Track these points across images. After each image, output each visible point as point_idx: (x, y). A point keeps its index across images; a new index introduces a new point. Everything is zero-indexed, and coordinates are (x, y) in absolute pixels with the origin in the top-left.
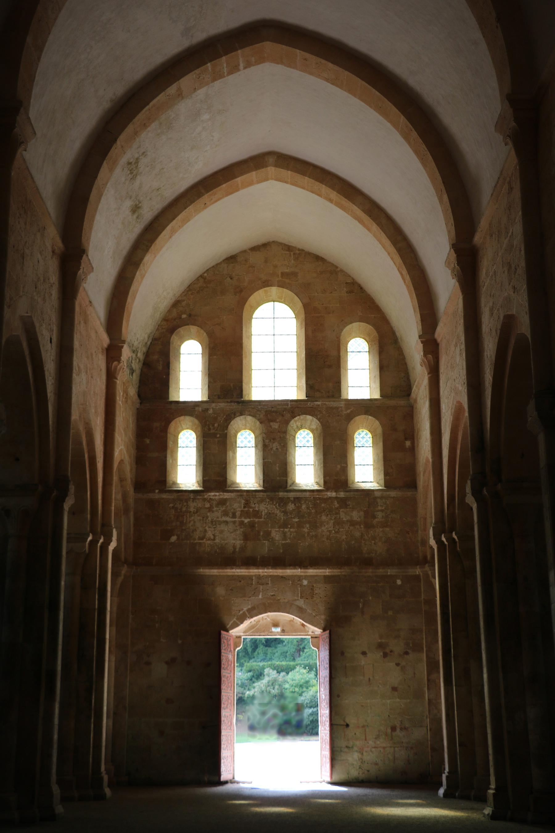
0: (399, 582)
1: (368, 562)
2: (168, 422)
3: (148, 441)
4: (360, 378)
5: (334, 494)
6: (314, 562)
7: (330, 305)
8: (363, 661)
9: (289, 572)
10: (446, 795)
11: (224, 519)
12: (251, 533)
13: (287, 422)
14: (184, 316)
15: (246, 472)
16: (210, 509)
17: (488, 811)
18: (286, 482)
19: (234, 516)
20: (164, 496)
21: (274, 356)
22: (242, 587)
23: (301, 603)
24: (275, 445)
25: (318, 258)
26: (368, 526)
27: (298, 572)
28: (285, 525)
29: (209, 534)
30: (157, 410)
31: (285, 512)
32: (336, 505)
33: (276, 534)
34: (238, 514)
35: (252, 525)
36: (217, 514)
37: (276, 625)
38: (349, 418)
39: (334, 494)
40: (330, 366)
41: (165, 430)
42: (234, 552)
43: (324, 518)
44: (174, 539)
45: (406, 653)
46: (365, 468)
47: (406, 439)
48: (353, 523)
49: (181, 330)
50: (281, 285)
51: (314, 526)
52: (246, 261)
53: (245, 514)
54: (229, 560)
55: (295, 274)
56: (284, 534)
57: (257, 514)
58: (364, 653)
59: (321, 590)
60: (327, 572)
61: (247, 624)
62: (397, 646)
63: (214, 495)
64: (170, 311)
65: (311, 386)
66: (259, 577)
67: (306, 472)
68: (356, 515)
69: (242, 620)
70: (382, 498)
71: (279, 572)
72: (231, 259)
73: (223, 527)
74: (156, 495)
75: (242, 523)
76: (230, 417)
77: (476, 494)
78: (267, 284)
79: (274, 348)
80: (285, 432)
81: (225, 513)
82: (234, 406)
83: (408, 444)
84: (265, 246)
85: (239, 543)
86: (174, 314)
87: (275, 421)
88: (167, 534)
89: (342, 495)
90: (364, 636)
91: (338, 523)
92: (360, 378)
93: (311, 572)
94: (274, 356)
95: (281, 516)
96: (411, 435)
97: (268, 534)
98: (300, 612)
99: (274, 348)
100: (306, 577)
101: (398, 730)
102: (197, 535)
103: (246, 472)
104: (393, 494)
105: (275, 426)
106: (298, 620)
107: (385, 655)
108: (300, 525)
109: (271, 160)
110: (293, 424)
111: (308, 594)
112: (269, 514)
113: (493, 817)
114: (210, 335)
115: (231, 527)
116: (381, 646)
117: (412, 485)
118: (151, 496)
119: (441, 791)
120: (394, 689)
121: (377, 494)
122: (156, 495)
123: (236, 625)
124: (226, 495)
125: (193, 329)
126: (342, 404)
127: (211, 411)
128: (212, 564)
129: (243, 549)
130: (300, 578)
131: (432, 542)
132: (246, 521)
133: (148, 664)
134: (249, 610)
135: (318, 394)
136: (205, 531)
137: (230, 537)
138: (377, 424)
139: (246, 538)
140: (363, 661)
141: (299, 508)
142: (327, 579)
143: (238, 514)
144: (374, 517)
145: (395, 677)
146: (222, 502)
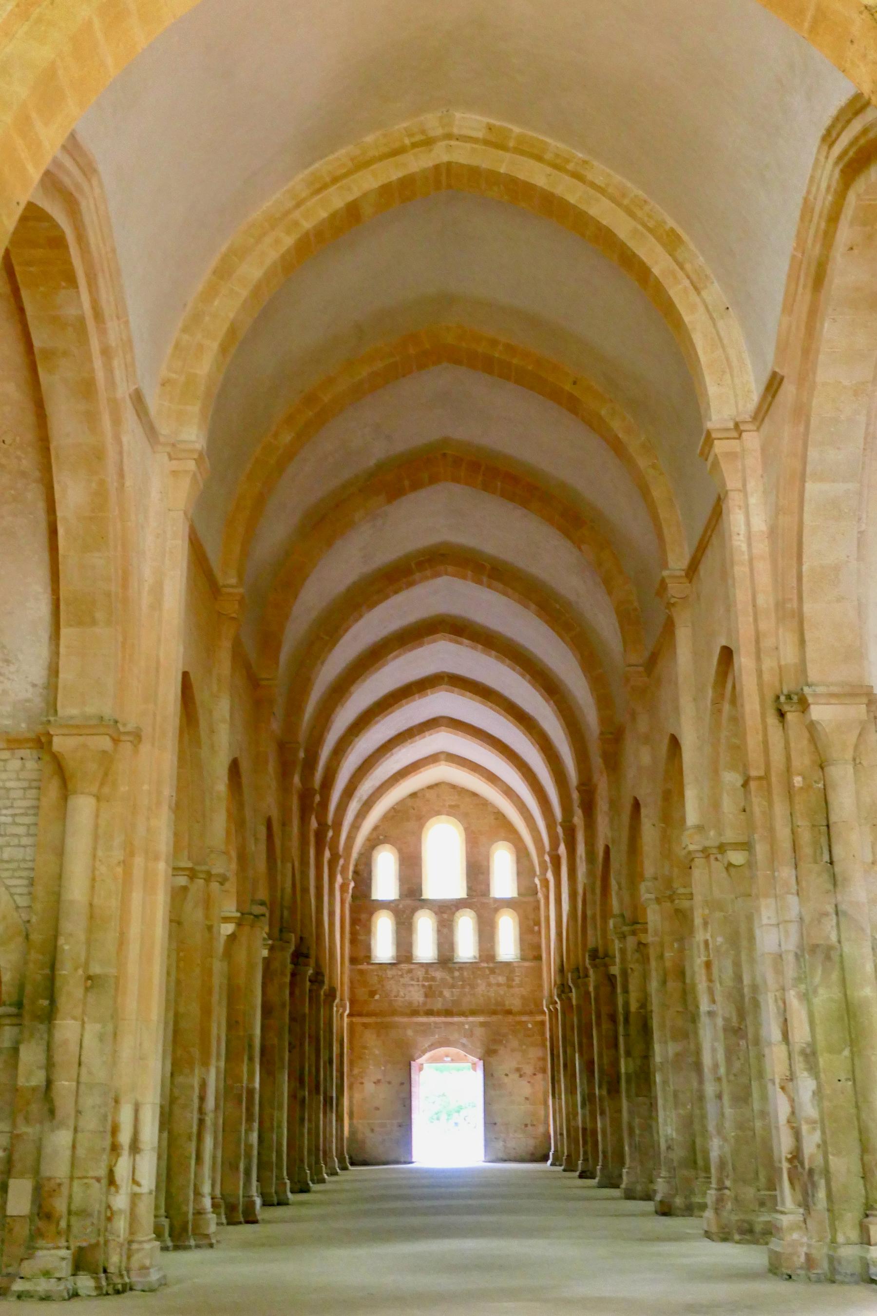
0: (530, 1026)
1: (509, 1012)
2: (371, 914)
3: (358, 928)
4: (504, 881)
5: (485, 965)
6: (473, 1013)
7: (484, 826)
8: (506, 1080)
9: (456, 1019)
10: (552, 1165)
11: (412, 983)
12: (430, 993)
13: (454, 914)
14: (381, 837)
15: (425, 948)
16: (402, 976)
17: (562, 1168)
18: (453, 956)
19: (418, 981)
20: (370, 967)
21: (444, 878)
22: (425, 1030)
23: (464, 1041)
24: (445, 931)
25: (475, 795)
26: (510, 987)
27: (462, 1019)
28: (453, 986)
29: (402, 994)
30: (363, 907)
31: (453, 978)
32: (487, 972)
33: (447, 993)
34: (421, 979)
35: (430, 987)
36: (406, 980)
37: (447, 1056)
38: (496, 910)
39: (485, 965)
40: (483, 873)
41: (369, 920)
42: (418, 1006)
43: (479, 981)
44: (377, 997)
45: (535, 1074)
46: (508, 945)
47: (535, 925)
48: (499, 985)
49: (380, 847)
50: (448, 814)
51: (473, 987)
52: (424, 796)
53: (426, 979)
54: (415, 1013)
55: (457, 806)
56: (452, 992)
57: (433, 979)
58: (507, 1075)
59: (479, 1032)
60: (481, 1019)
61: (428, 1055)
62: (528, 1069)
63: (405, 966)
64: (371, 833)
65: (470, 889)
66: (435, 1023)
67: (466, 948)
68: (501, 979)
69: (424, 1052)
70: (518, 967)
71: (449, 1019)
72: (414, 795)
73: (411, 988)
74: (364, 967)
75: (423, 986)
76: (414, 911)
77: (559, 996)
78: (438, 813)
79: (443, 846)
80: (452, 921)
81: (412, 979)
82: (417, 903)
83: (536, 928)
84: (437, 785)
85: (421, 999)
86: (374, 836)
87: (446, 912)
88: (372, 994)
89: (491, 965)
90: (507, 1062)
91: (489, 985)
92: (504, 881)
93: (471, 1019)
94: (444, 878)
95: (450, 980)
96: (538, 923)
97: (441, 993)
98: (463, 1047)
99: (443, 846)
100: (467, 1023)
101: (529, 1126)
102: (394, 994)
103: (425, 948)
104: (527, 964)
105: (445, 916)
106: (462, 1053)
107: (521, 1076)
108: (463, 987)
109: (443, 757)
110: (458, 914)
111: (470, 1034)
112: (442, 979)
113: (564, 1170)
114: (400, 851)
115: (416, 988)
116: (518, 1070)
117: (539, 958)
118: (360, 967)
119: (549, 1162)
120: (527, 1099)
121: (515, 965)
122: (364, 967)
123: (420, 1056)
124: (412, 966)
125: (387, 847)
126: (491, 901)
127: (401, 906)
128: (403, 1014)
129: (425, 1004)
130: (463, 1024)
131: (545, 1009)
132: (426, 984)
133: (362, 1083)
134: (429, 1046)
135: (474, 893)
136: (398, 991)
137: (416, 996)
138: (515, 914)
139: (426, 996)
140: (506, 1080)
141: (462, 974)
142: (482, 1024)
143: (421, 979)
144: (513, 980)
145: (527, 1090)
146: (410, 971)
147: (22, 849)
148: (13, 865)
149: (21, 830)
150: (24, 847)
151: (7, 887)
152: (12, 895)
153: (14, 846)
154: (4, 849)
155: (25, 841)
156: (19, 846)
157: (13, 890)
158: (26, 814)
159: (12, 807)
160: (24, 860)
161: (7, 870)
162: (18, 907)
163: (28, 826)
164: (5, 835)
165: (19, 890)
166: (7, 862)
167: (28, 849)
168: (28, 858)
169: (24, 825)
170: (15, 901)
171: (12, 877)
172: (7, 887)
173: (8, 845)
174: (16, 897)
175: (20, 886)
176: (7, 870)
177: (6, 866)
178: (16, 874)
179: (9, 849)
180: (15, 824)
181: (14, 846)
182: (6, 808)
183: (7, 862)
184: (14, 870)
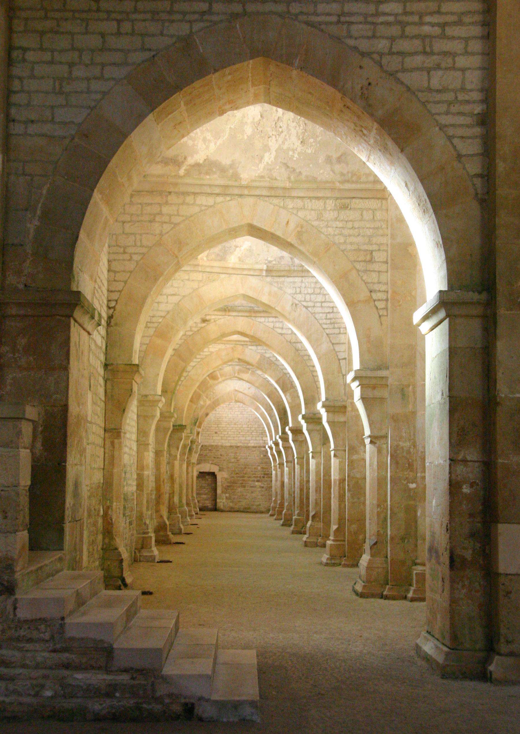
147: (459, 73)
148: (450, 96)
149: (457, 46)
150: (463, 70)
151: (442, 127)
152: (450, 138)
153: (446, 69)
154: (432, 73)
155: (462, 62)
156: (454, 68)
157: (451, 132)
158: (459, 23)
159: (439, 12)
160: (463, 89)
161: (438, 102)
162: (459, 156)
163: (466, 40)
164: (432, 53)
165: (459, 132)
166: (438, 91)
167: (468, 73)
168: (468, 86)
169: (460, 38)
170: (455, 147)
171: (447, 113)
172: (442, 127)
173: (438, 67)
174: (456, 141)
175: (460, 126)
176: (438, 102)
177: (438, 97)
178: (454, 109)
179: (440, 73)
180: (443, 36)
181: (446, 69)
182: (431, 14)
183: (438, 91)
184: (450, 103)
